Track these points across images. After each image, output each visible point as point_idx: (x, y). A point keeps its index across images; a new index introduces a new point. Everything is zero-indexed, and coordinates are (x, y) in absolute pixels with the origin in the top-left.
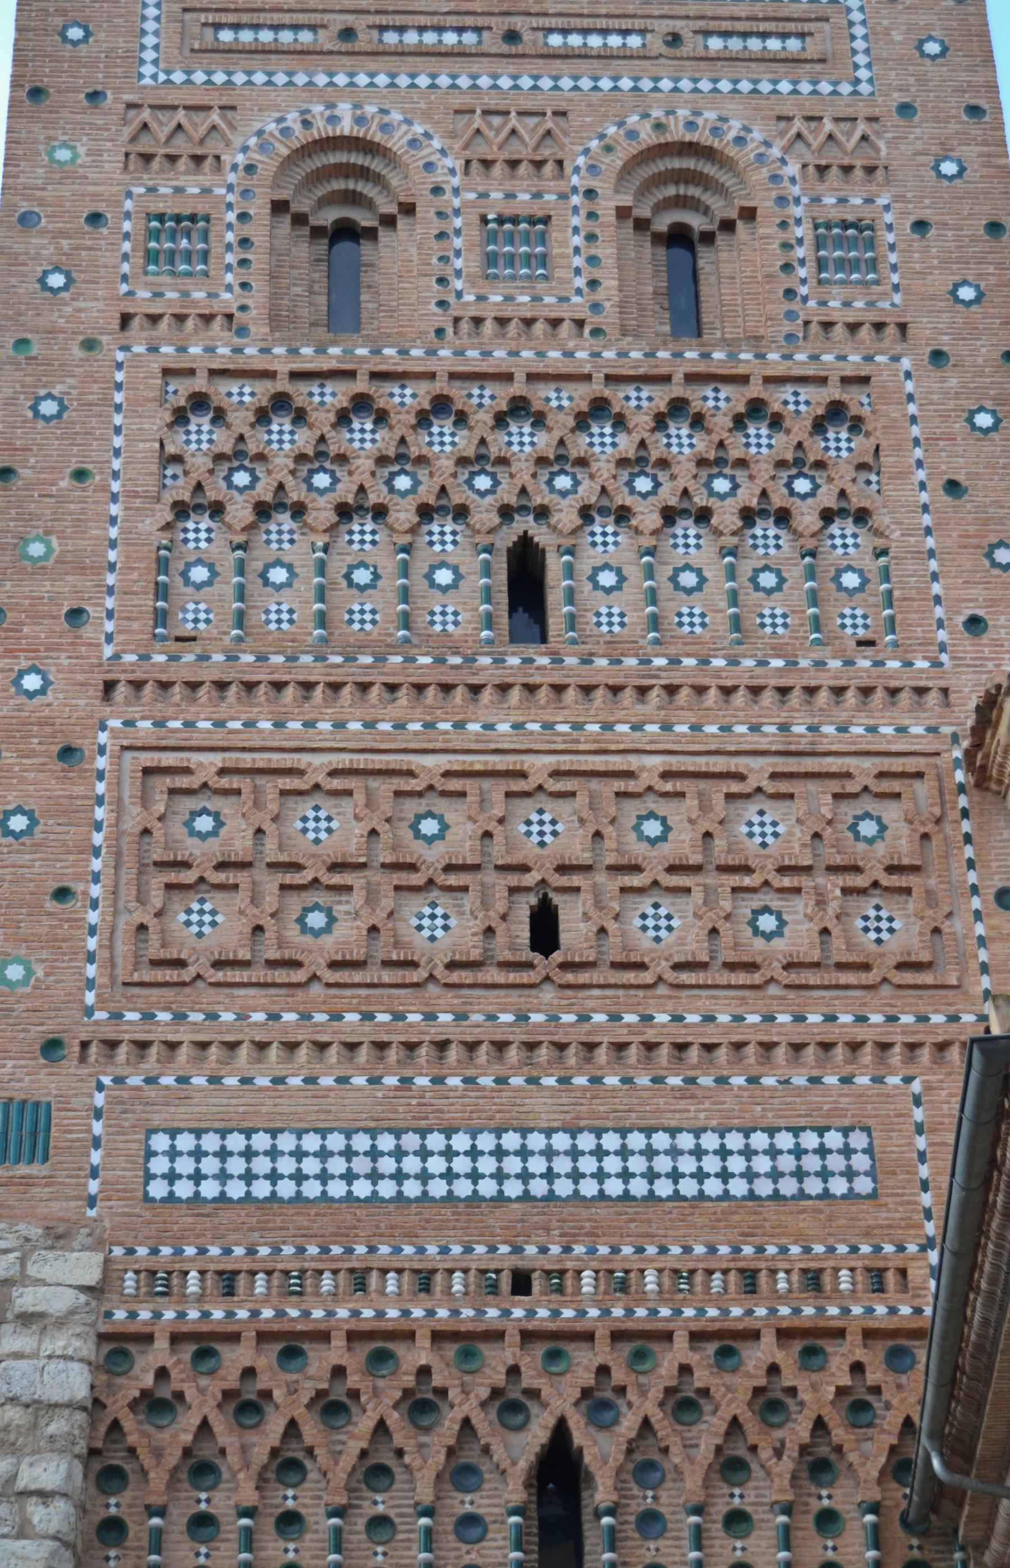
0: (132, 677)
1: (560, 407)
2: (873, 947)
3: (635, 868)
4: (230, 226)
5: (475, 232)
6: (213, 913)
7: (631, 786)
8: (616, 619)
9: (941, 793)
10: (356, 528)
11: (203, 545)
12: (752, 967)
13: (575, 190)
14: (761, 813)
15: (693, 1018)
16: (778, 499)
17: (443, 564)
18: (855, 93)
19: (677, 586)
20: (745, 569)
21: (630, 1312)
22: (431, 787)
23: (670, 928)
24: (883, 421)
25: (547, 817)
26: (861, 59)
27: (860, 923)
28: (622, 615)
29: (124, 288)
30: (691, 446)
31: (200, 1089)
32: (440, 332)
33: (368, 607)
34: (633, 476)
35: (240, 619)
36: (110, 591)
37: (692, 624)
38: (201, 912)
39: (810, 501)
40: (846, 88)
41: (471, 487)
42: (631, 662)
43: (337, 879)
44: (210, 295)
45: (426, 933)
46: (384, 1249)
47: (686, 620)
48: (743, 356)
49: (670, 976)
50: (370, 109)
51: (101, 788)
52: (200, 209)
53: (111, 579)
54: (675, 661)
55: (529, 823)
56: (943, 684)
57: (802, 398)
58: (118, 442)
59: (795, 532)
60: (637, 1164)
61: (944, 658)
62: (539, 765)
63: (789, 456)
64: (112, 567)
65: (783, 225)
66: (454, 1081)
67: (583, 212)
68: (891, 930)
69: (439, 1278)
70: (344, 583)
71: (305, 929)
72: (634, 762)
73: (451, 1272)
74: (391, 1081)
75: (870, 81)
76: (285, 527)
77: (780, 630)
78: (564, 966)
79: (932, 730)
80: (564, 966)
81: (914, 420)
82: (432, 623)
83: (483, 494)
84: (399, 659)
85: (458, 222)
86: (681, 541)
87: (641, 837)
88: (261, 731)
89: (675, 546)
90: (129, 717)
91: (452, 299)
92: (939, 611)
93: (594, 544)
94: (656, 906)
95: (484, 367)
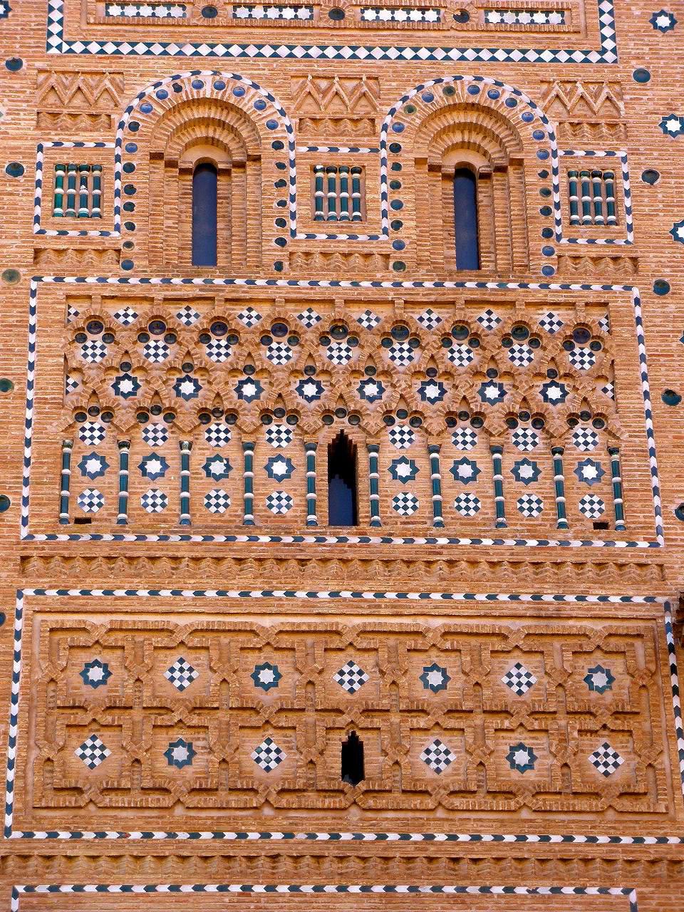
0: (43, 553)
1: (370, 327)
2: (603, 778)
4: (118, 176)
5: (307, 182)
6: (102, 748)
7: (420, 642)
8: (410, 504)
9: (656, 653)
11: (97, 441)
12: (509, 794)
13: (383, 144)
14: (518, 666)
15: (464, 838)
17: (279, 458)
18: (602, 61)
20: (508, 461)
23: (447, 762)
24: (618, 340)
26: (607, 32)
27: (592, 759)
28: (414, 500)
29: (37, 228)
30: (469, 359)
31: (91, 895)
32: (279, 266)
33: (222, 493)
35: (123, 505)
36: (26, 482)
37: (467, 508)
38: (93, 747)
40: (594, 57)
41: (301, 393)
44: (103, 234)
45: (263, 765)
48: (511, 285)
50: (227, 75)
51: (18, 646)
52: (95, 161)
53: (26, 472)
54: (454, 541)
55: (342, 673)
56: (658, 561)
58: (32, 357)
59: (548, 432)
61: (660, 539)
64: (27, 462)
65: (544, 175)
66: (283, 889)
67: (389, 163)
68: (616, 765)
70: (204, 473)
71: (171, 761)
75: (614, 51)
76: (160, 427)
77: (535, 513)
79: (650, 599)
81: (641, 339)
82: (271, 506)
83: (310, 399)
84: (245, 538)
85: (293, 172)
86: (460, 439)
88: (140, 598)
90: (39, 587)
91: (288, 238)
92: (657, 501)
95: (313, 295)
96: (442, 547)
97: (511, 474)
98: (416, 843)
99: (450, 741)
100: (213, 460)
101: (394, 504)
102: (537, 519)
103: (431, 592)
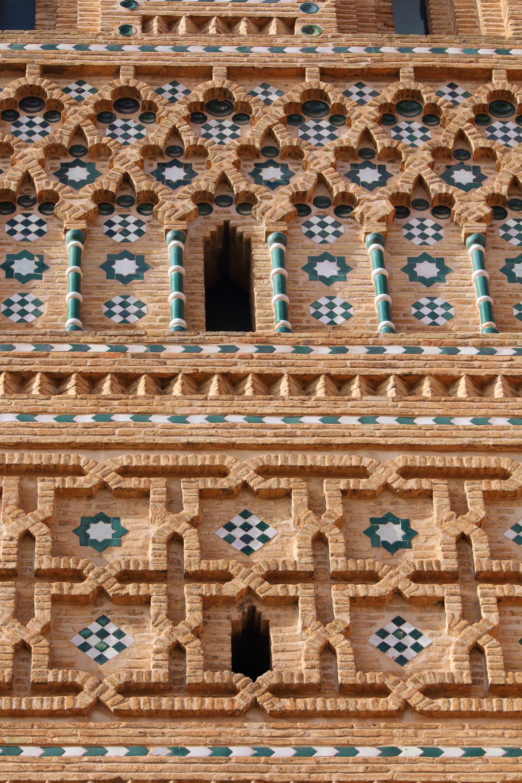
7: (363, 484)
10: (19, 218)
20: (498, 259)
22: (104, 486)
32: (125, 30)
34: (356, 167)
41: (161, 178)
45: (93, 653)
54: (413, 350)
78: (279, 691)
80: (279, 691)
82: (110, 314)
84: (67, 347)
86: (416, 232)
89: (410, 236)
93: (311, 235)
94: (399, 621)
95: (178, 61)
97: (501, 274)
98: (366, 761)
99: (421, 619)
100: (20, 257)
101: (312, 311)
103: (377, 415)
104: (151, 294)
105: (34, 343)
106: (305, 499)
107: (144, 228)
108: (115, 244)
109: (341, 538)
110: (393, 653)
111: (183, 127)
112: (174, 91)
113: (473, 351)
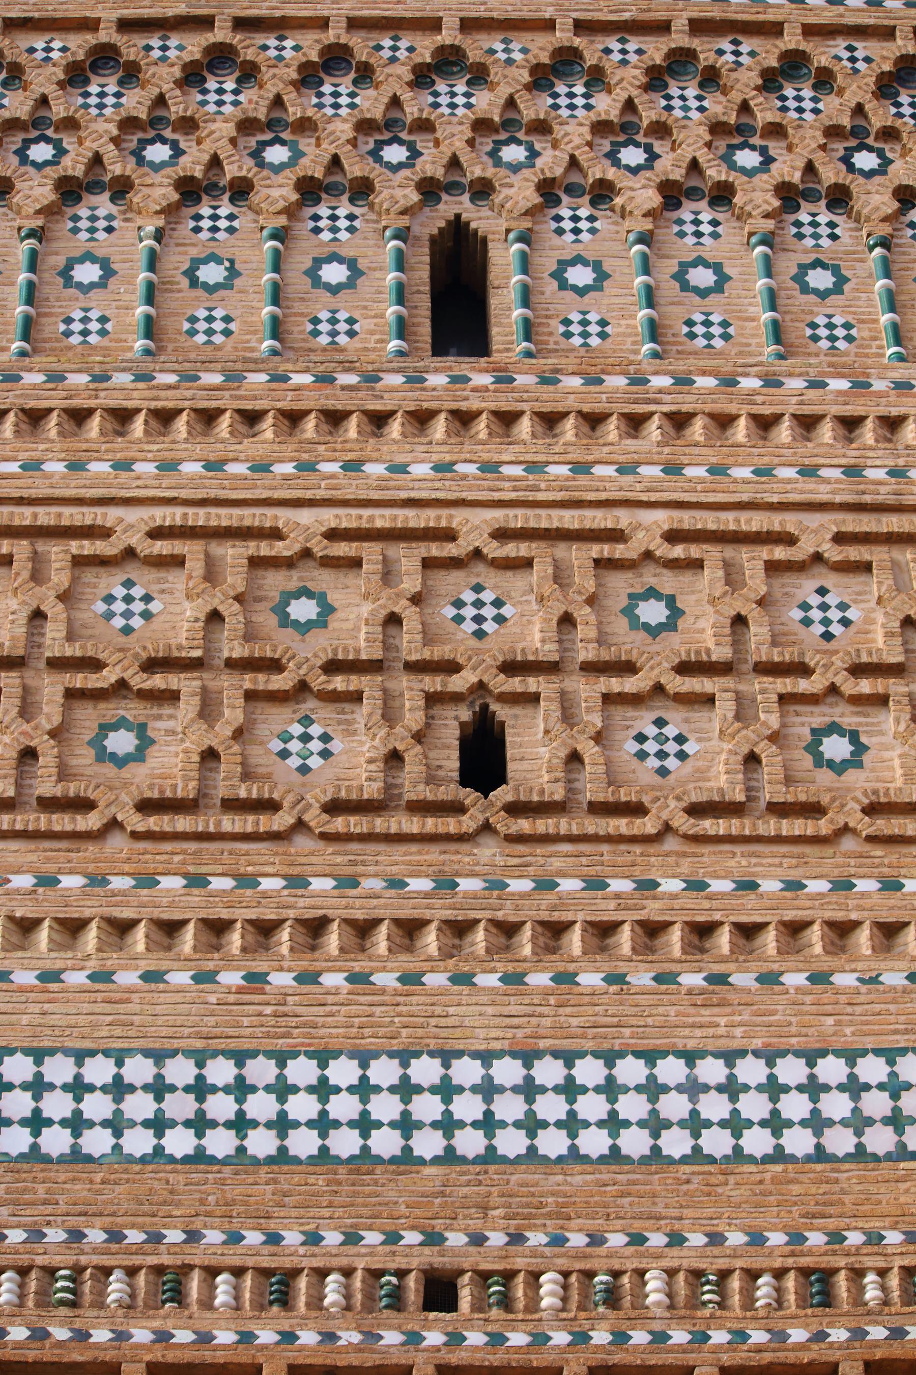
3: (629, 668)
7: (619, 551)
10: (206, 211)
12: (814, 810)
14: (822, 591)
16: (830, 173)
17: (334, 258)
19: (685, 287)
20: (788, 265)
21: (620, 1337)
23: (682, 756)
25: (487, 596)
30: (701, 109)
33: (218, 313)
39: (877, 179)
41: (379, 159)
42: (617, 382)
43: (158, 681)
45: (294, 762)
46: (214, 1237)
47: (699, 330)
49: (682, 822)
54: (683, 381)
57: (859, 54)
60: (632, 1107)
62: (474, 528)
63: (846, 121)
69: (302, 1283)
70: (185, 282)
72: (623, 518)
73: (322, 1274)
74: (232, 978)
77: (841, 345)
78: (515, 809)
80: (515, 809)
82: (316, 333)
84: (264, 377)
87: (635, 624)
88: (49, 476)
89: (682, 234)
93: (560, 232)
94: (660, 723)
96: (660, 391)
97: (791, 284)
98: (617, 896)
99: (687, 721)
100: (206, 261)
101: (562, 329)
102: (846, 354)
103: (639, 464)
104: (365, 308)
105: (223, 371)
106: (550, 571)
107: (356, 223)
108: (322, 244)
109: (593, 619)
110: (653, 763)
111: (406, 95)
112: (394, 49)
113: (756, 383)
